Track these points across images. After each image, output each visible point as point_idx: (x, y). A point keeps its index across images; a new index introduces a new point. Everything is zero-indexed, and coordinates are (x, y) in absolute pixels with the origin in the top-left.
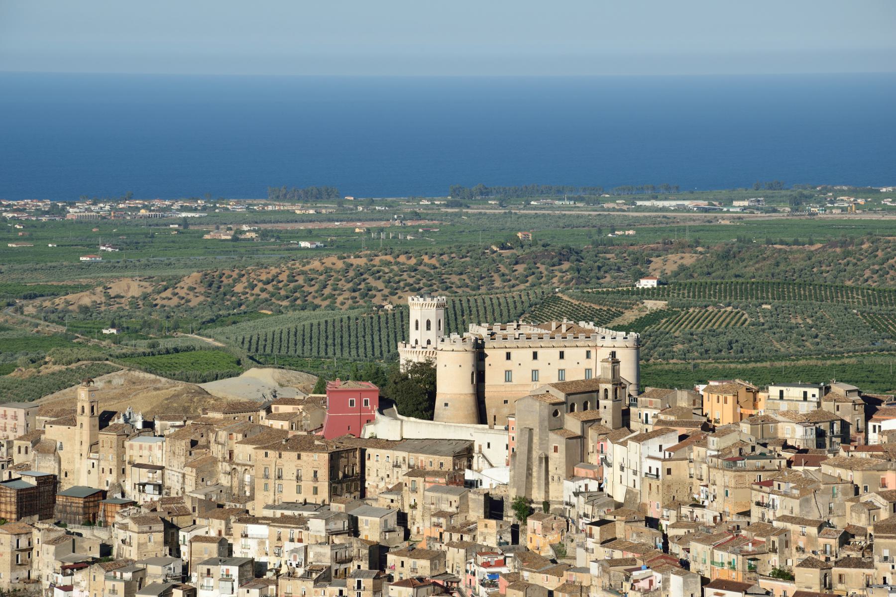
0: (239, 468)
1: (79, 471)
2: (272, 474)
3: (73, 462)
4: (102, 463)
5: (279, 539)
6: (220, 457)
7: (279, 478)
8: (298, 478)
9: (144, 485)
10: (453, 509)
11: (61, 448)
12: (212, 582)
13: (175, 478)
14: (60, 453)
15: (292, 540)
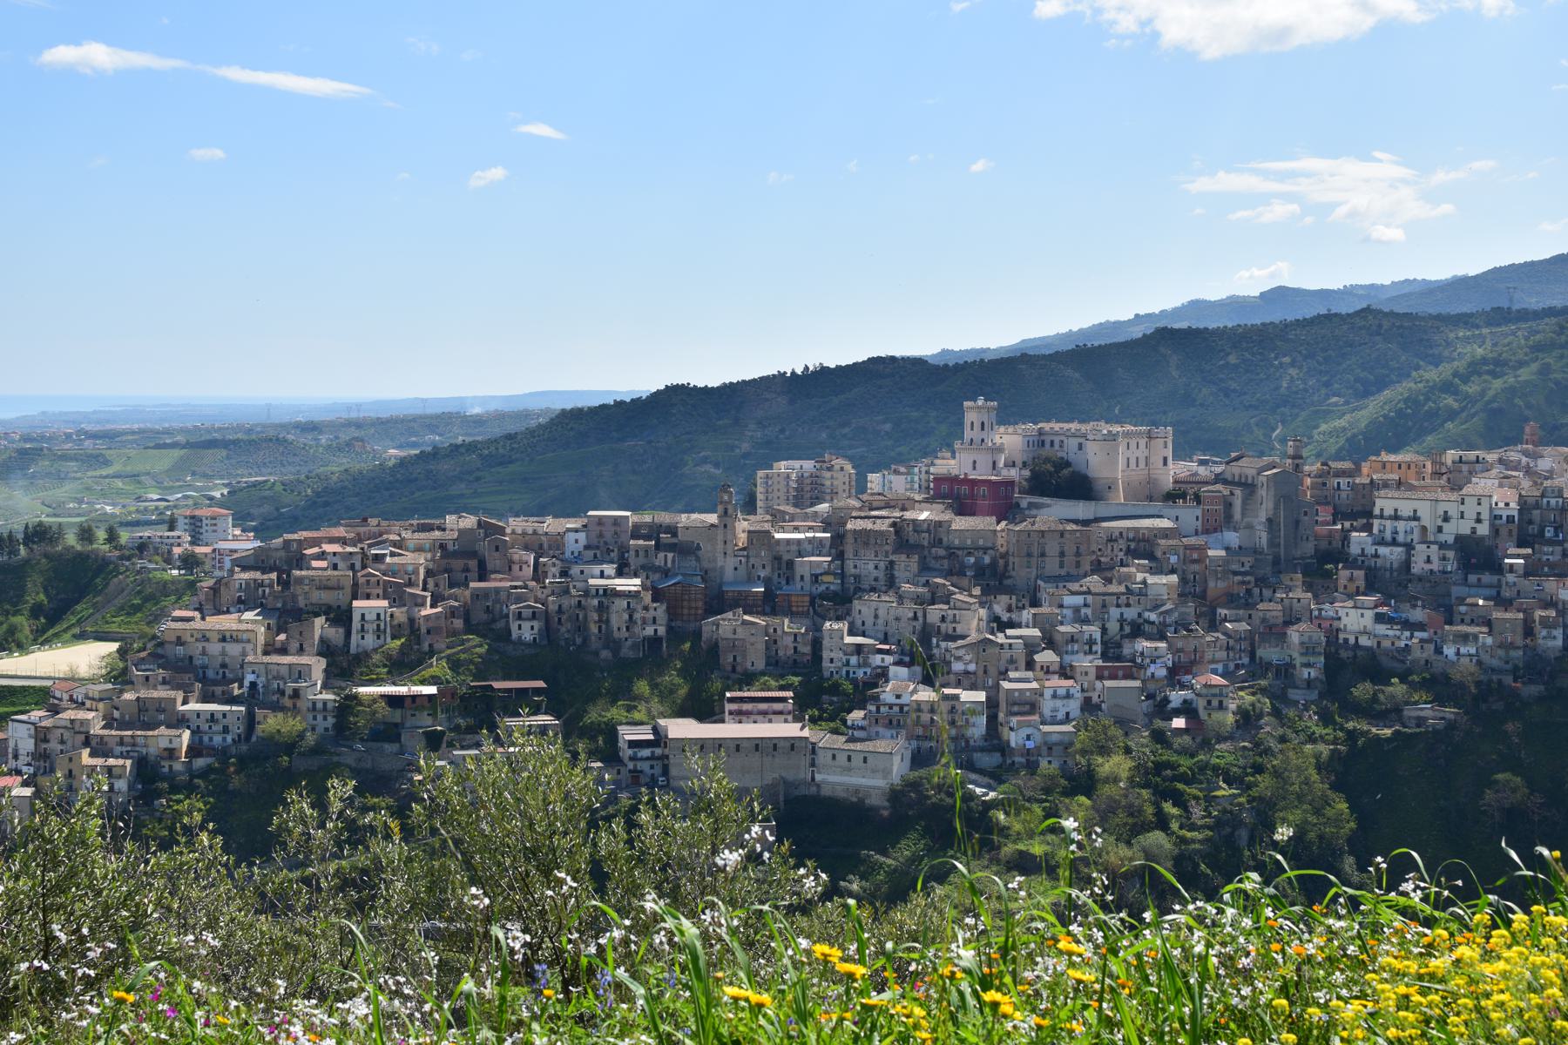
0: (960, 553)
1: (722, 568)
2: (1035, 551)
3: (715, 560)
4: (752, 561)
5: (1104, 606)
6: (926, 543)
7: (1043, 555)
8: (1062, 554)
9: (816, 576)
10: (1247, 568)
11: (698, 548)
12: (1076, 647)
13: (871, 566)
14: (700, 553)
15: (1118, 606)
